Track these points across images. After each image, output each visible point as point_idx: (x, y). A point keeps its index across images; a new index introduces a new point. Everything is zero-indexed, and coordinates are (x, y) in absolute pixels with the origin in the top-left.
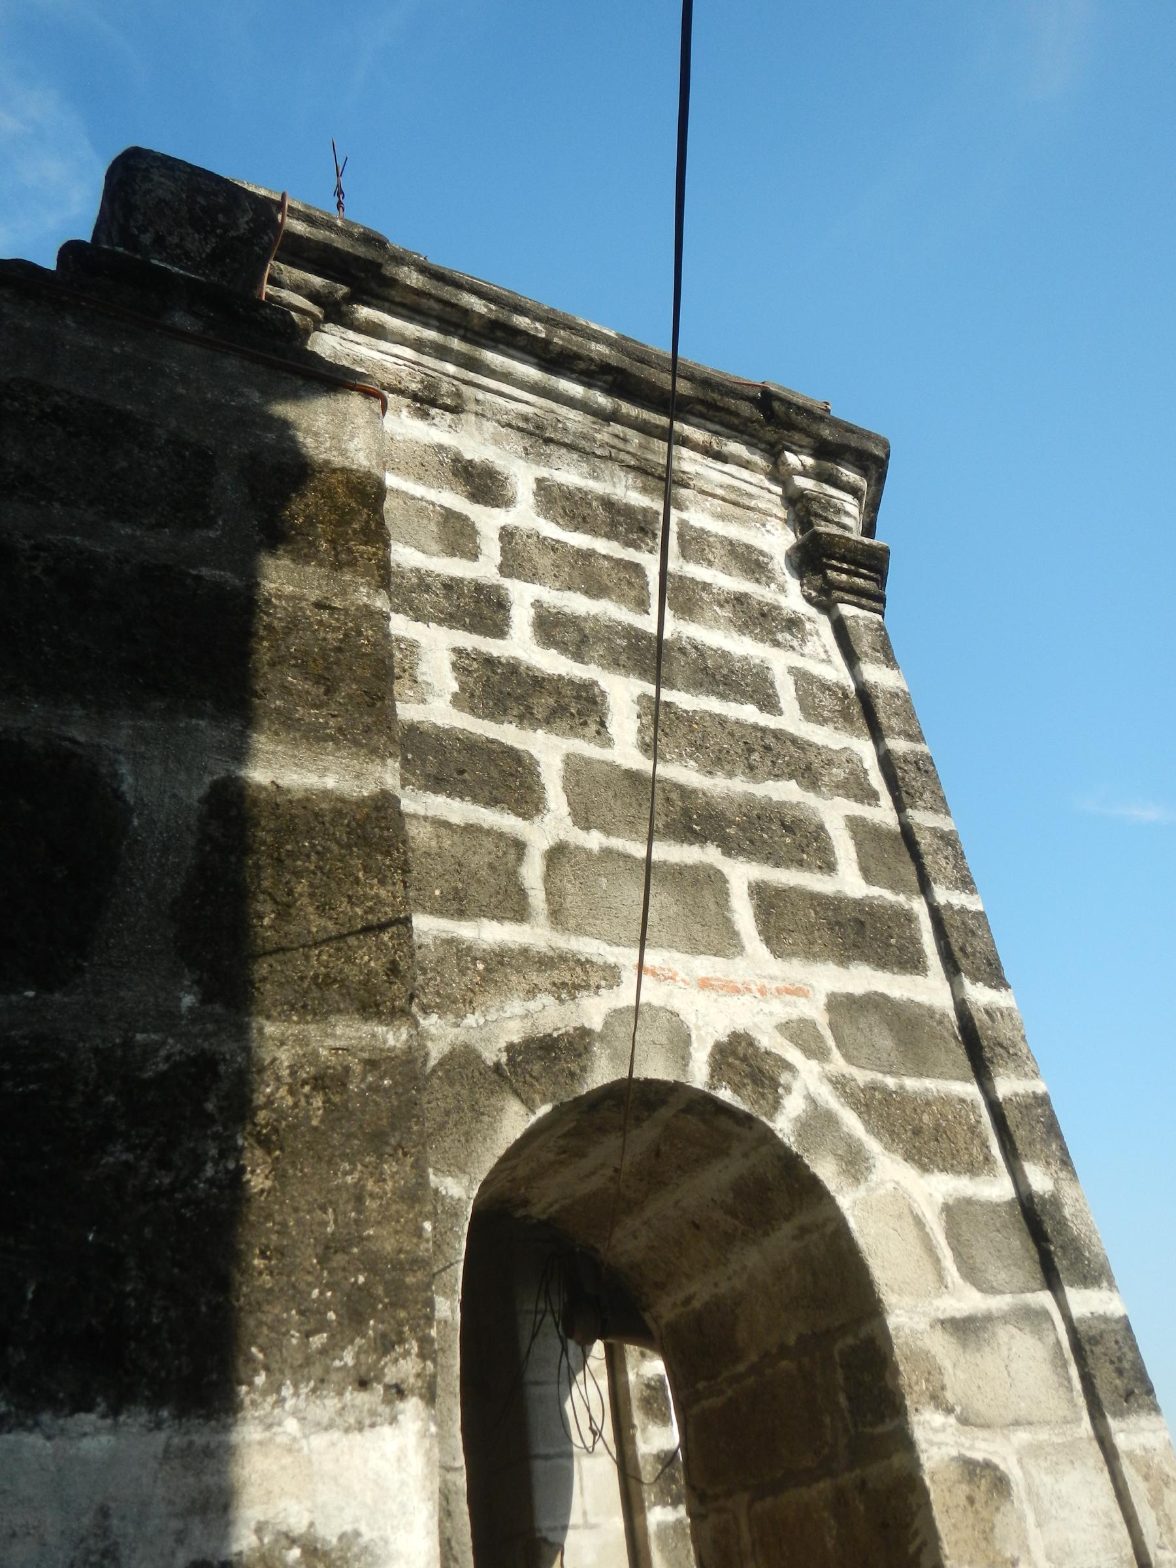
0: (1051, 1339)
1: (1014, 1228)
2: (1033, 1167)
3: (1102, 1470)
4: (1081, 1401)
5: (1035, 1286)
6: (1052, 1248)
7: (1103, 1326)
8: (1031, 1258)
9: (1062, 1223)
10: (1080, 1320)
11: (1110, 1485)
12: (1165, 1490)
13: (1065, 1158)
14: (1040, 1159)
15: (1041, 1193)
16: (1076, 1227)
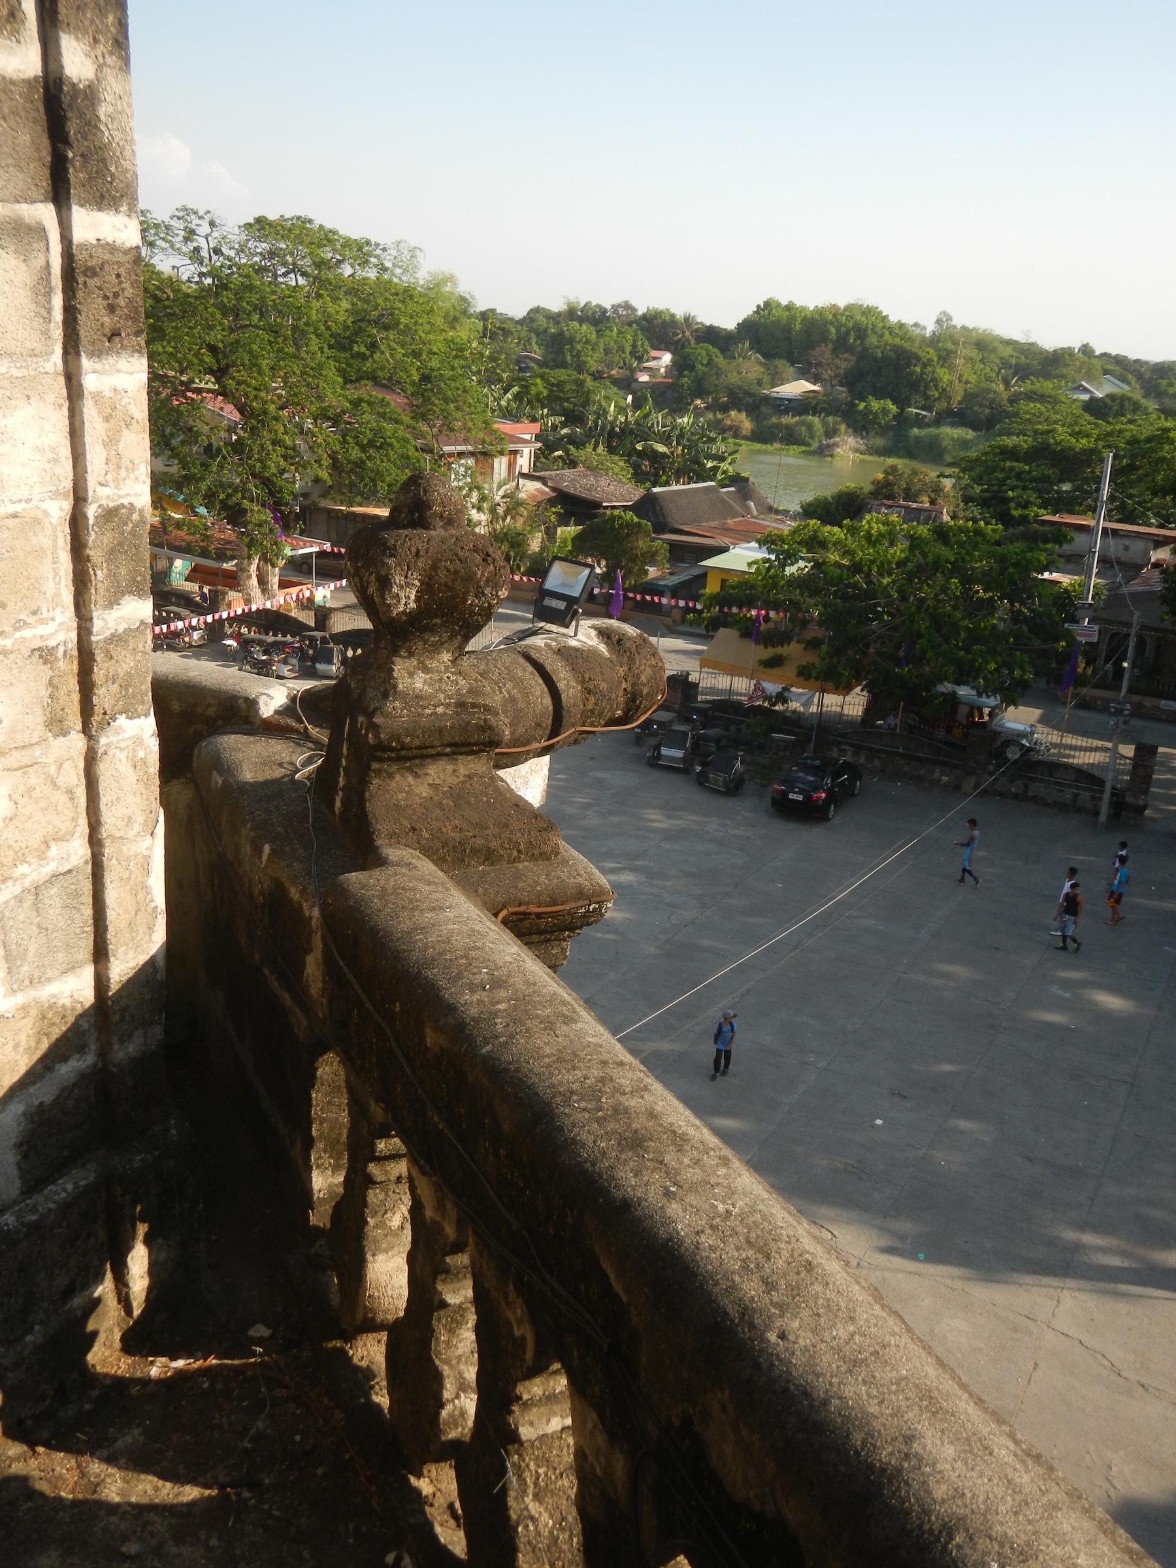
0: (41, 262)
1: (27, 117)
2: (74, 43)
3: (61, 406)
4: (57, 333)
5: (35, 196)
6: (70, 155)
7: (107, 256)
8: (41, 159)
9: (92, 124)
10: (83, 246)
11: (67, 422)
12: (125, 431)
13: (120, 39)
14: (87, 33)
15: (75, 81)
16: (109, 132)
